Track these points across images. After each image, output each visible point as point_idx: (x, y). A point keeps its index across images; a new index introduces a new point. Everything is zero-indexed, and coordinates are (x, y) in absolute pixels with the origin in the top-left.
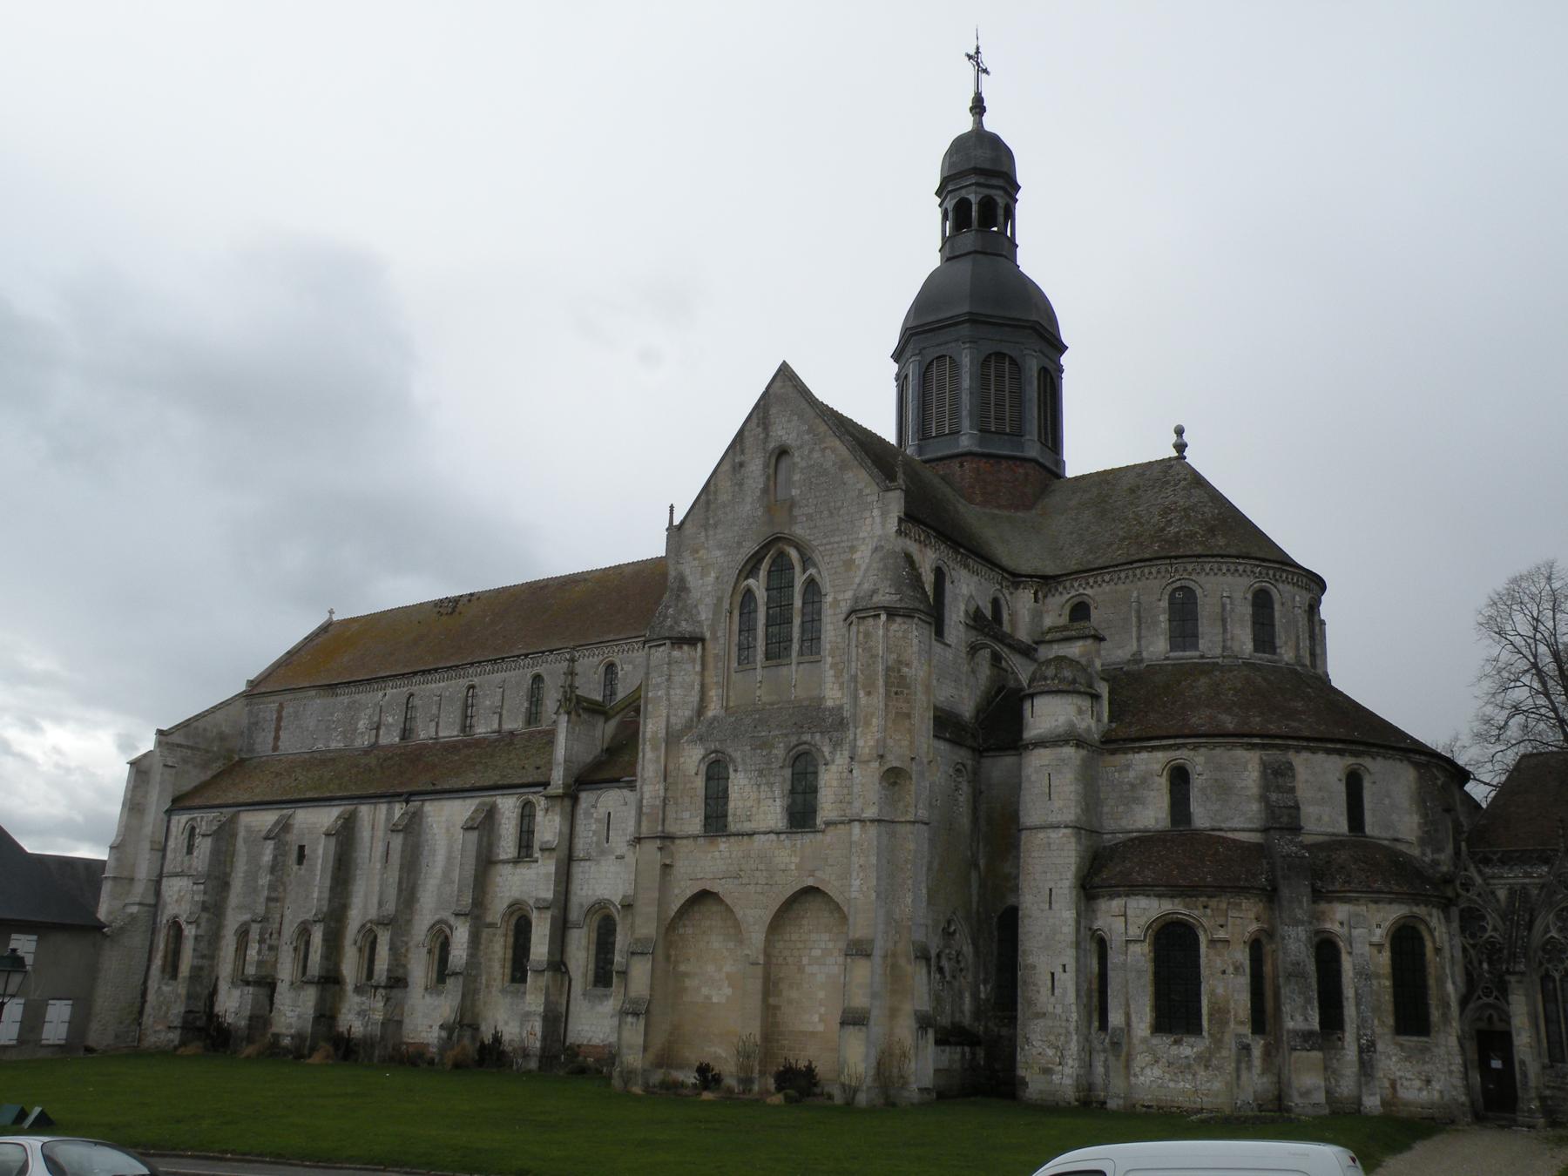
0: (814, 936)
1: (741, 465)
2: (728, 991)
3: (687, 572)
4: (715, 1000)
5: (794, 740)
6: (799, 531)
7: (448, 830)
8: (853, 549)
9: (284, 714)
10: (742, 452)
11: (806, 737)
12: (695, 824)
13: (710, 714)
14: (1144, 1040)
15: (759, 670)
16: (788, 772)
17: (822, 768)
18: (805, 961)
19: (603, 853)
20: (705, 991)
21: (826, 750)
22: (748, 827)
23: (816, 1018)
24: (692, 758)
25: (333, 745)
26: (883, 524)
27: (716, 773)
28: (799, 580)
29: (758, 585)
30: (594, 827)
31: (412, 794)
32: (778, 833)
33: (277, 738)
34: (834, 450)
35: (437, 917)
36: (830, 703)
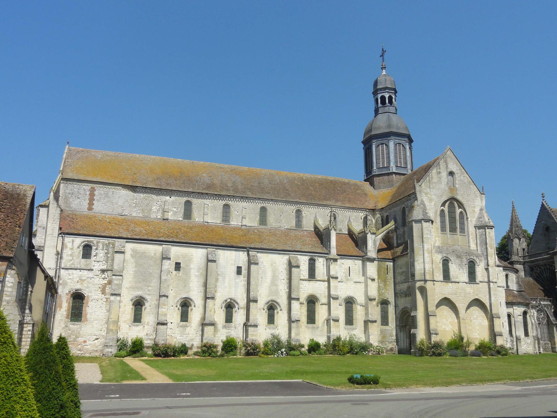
0: (474, 312)
1: (440, 172)
2: (451, 327)
3: (424, 200)
4: (447, 329)
5: (468, 258)
6: (459, 198)
7: (272, 265)
8: (474, 207)
9: (96, 193)
10: (440, 168)
11: (472, 257)
12: (441, 278)
13: (437, 245)
14: (523, 338)
15: (449, 236)
16: (467, 266)
17: (476, 266)
18: (472, 318)
19: (348, 280)
20: (443, 327)
21: (478, 261)
22: (457, 280)
23: (477, 334)
24: (438, 258)
25: (134, 214)
26: (482, 203)
27: (446, 262)
28: (458, 211)
29: (446, 209)
30: (343, 271)
31: (251, 248)
32: (466, 283)
33: (91, 204)
34: (467, 178)
35: (270, 299)
36: (472, 248)
